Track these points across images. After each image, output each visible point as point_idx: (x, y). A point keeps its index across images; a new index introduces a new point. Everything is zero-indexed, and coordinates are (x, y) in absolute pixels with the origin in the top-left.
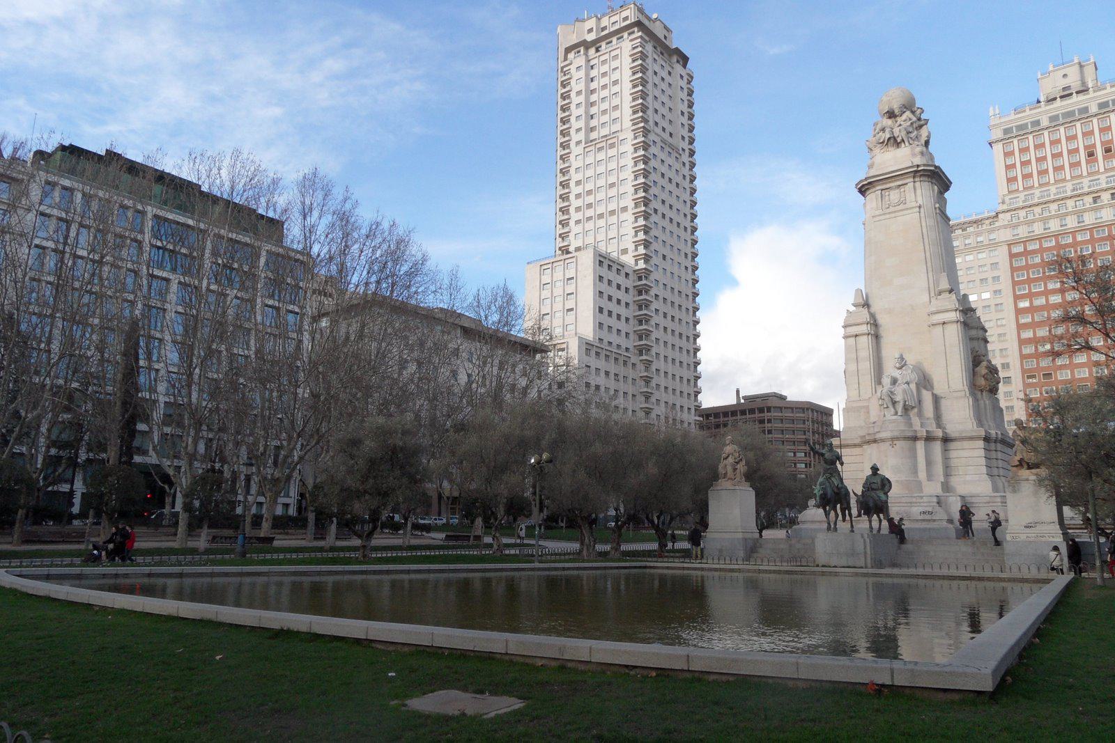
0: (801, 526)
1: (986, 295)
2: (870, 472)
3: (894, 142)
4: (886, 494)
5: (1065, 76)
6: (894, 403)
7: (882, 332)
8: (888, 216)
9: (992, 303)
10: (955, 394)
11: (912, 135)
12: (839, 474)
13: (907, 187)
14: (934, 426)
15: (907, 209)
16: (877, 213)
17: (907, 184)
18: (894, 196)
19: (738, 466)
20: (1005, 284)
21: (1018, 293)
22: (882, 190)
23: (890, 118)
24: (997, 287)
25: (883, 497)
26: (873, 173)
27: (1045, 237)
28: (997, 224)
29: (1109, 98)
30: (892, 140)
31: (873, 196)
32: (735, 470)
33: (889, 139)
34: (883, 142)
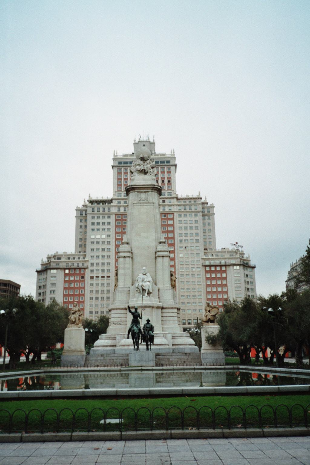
0: (95, 348)
1: (104, 236)
2: (146, 322)
3: (144, 172)
4: (153, 332)
5: (144, 145)
6: (144, 290)
7: (134, 257)
8: (140, 204)
9: (106, 240)
10: (166, 288)
11: (150, 171)
12: (139, 323)
13: (148, 193)
14: (158, 302)
15: (149, 203)
16: (135, 202)
17: (149, 192)
18: (143, 196)
19: (80, 318)
20: (112, 233)
21: (117, 237)
22: (138, 192)
23: (142, 160)
24: (109, 233)
25: (153, 334)
26: (133, 183)
27: (124, 214)
28: (112, 204)
29: (159, 160)
30: (143, 171)
31: (132, 195)
32: (79, 319)
33: (142, 170)
34: (139, 171)
